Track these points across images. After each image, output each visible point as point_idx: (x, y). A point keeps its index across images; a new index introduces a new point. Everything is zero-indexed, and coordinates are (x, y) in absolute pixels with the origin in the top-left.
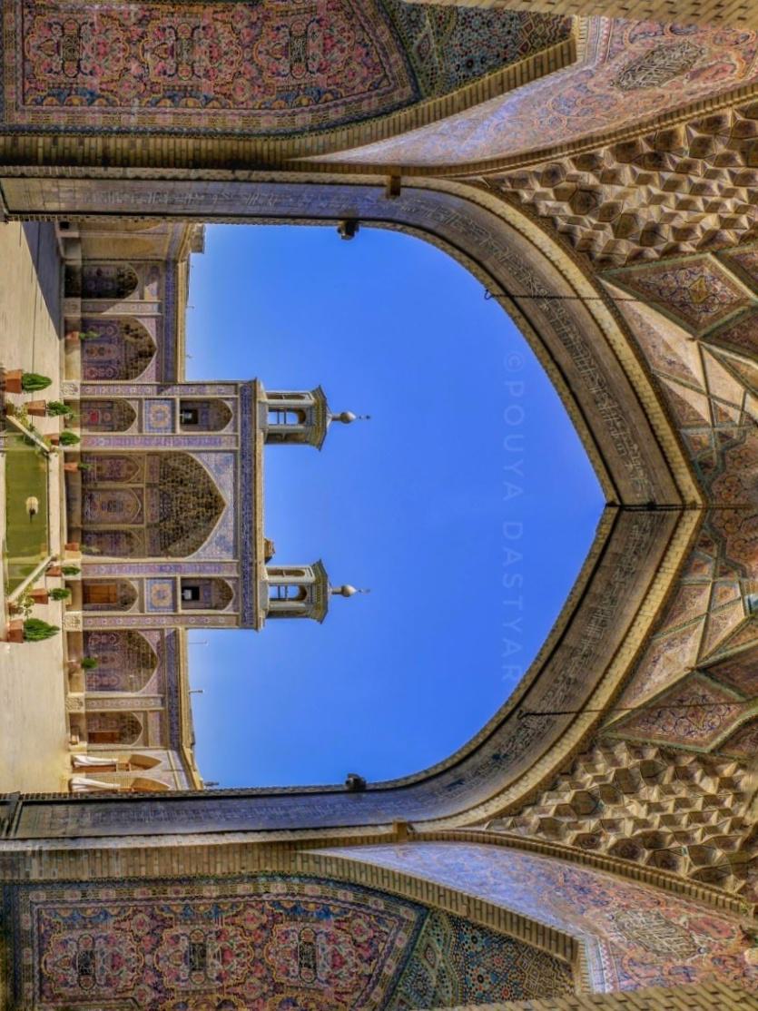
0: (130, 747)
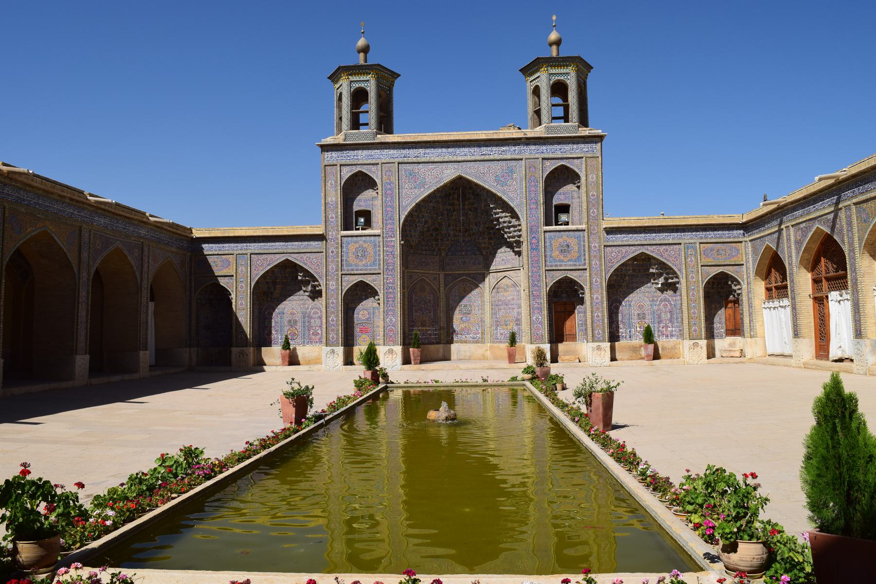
0: (744, 286)
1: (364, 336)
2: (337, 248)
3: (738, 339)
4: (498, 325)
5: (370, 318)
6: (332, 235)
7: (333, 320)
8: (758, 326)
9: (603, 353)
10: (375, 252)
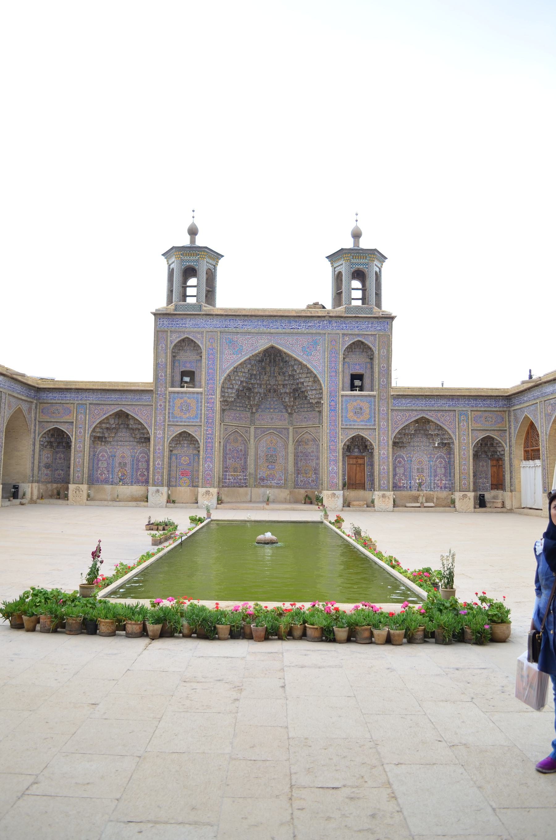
0: (507, 449)
1: (185, 478)
2: (165, 402)
3: (500, 492)
4: (298, 474)
5: (190, 462)
6: (161, 391)
7: (158, 464)
8: (516, 481)
9: (387, 500)
10: (197, 407)
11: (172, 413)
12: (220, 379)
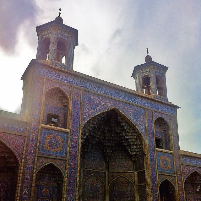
5: (50, 194)
7: (25, 194)
10: (64, 145)
11: (42, 146)
12: (82, 124)
